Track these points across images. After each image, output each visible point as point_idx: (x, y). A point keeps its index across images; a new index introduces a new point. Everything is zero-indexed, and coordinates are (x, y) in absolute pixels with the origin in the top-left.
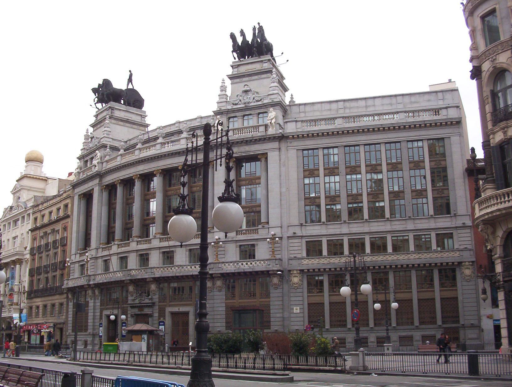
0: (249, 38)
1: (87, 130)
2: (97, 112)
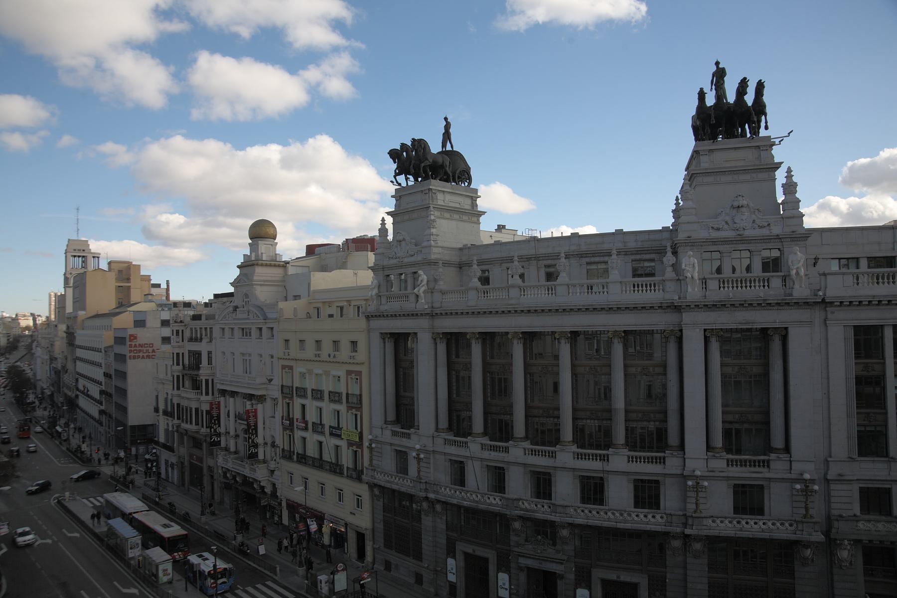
1: (383, 220)
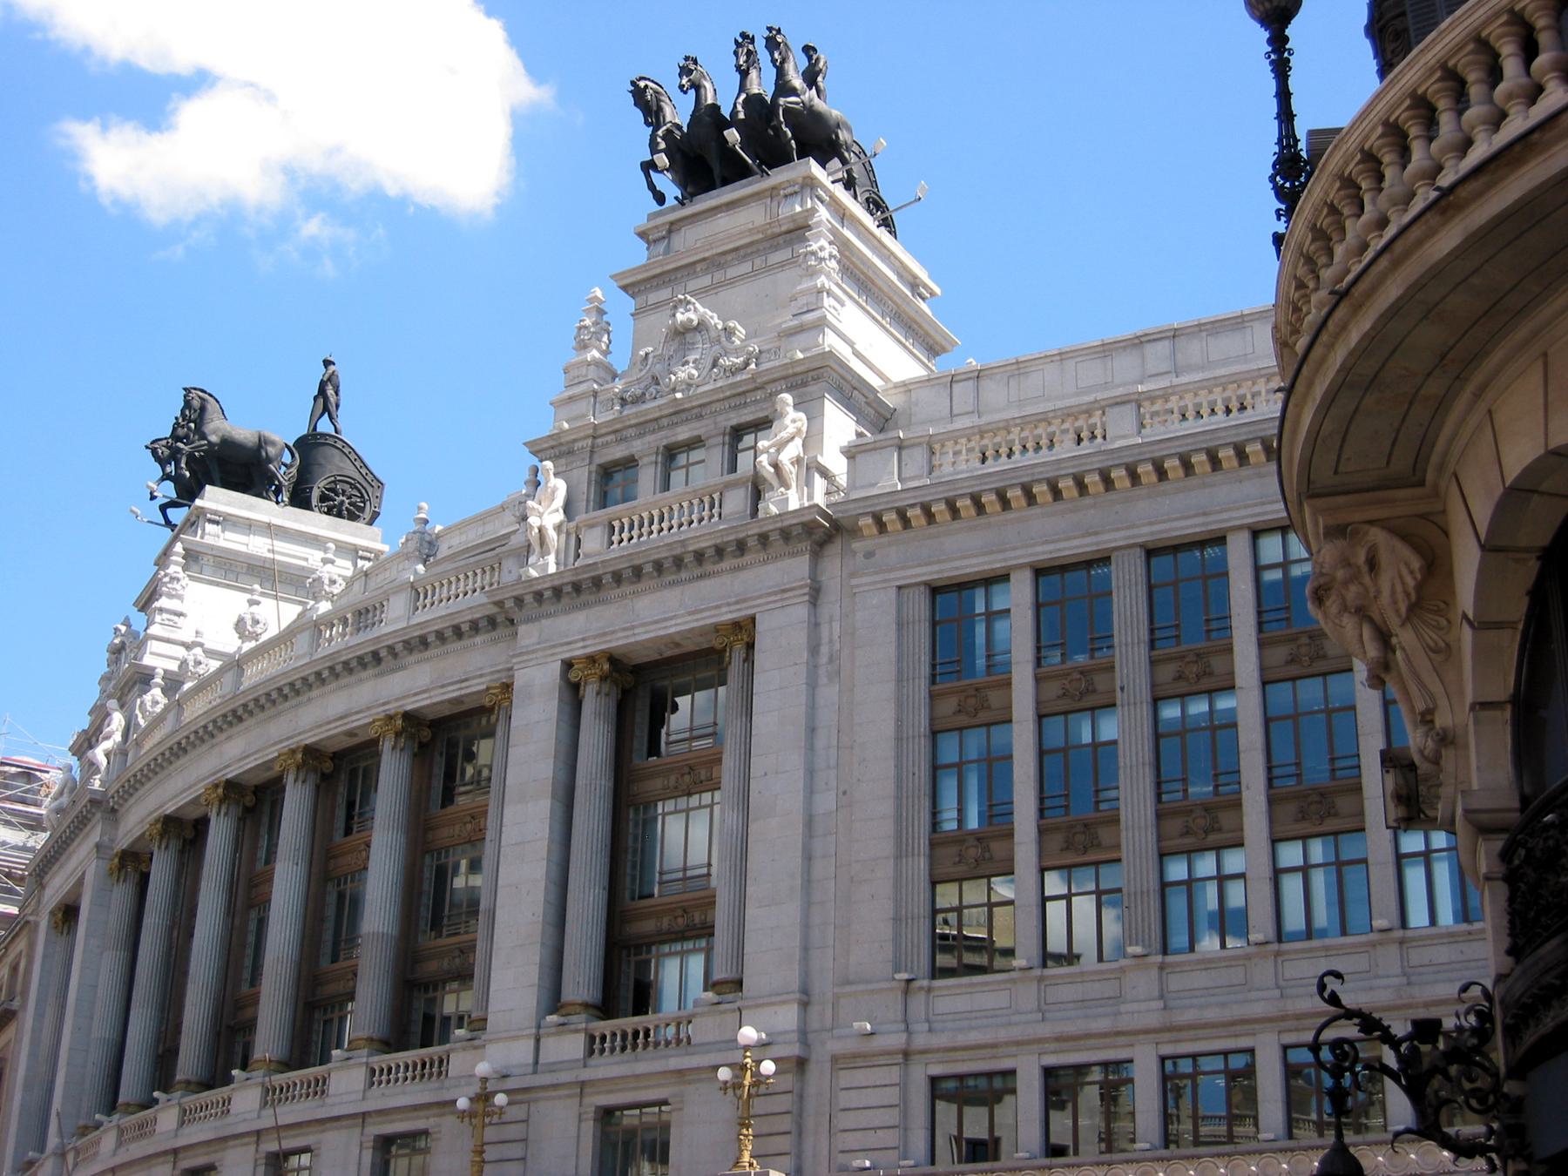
0: (724, 94)
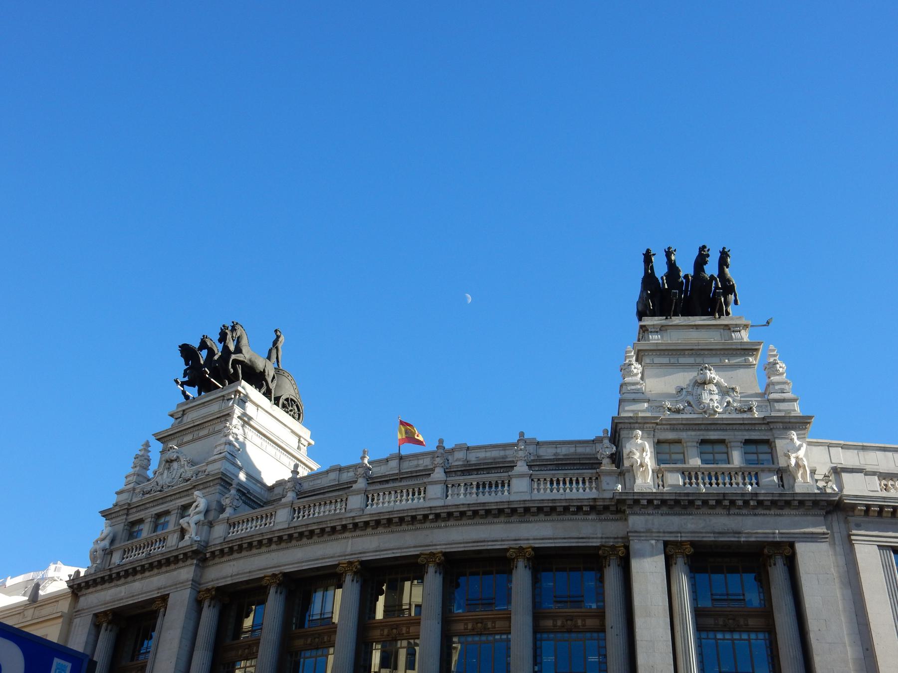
0: (686, 269)
1: (147, 445)
2: (179, 406)
